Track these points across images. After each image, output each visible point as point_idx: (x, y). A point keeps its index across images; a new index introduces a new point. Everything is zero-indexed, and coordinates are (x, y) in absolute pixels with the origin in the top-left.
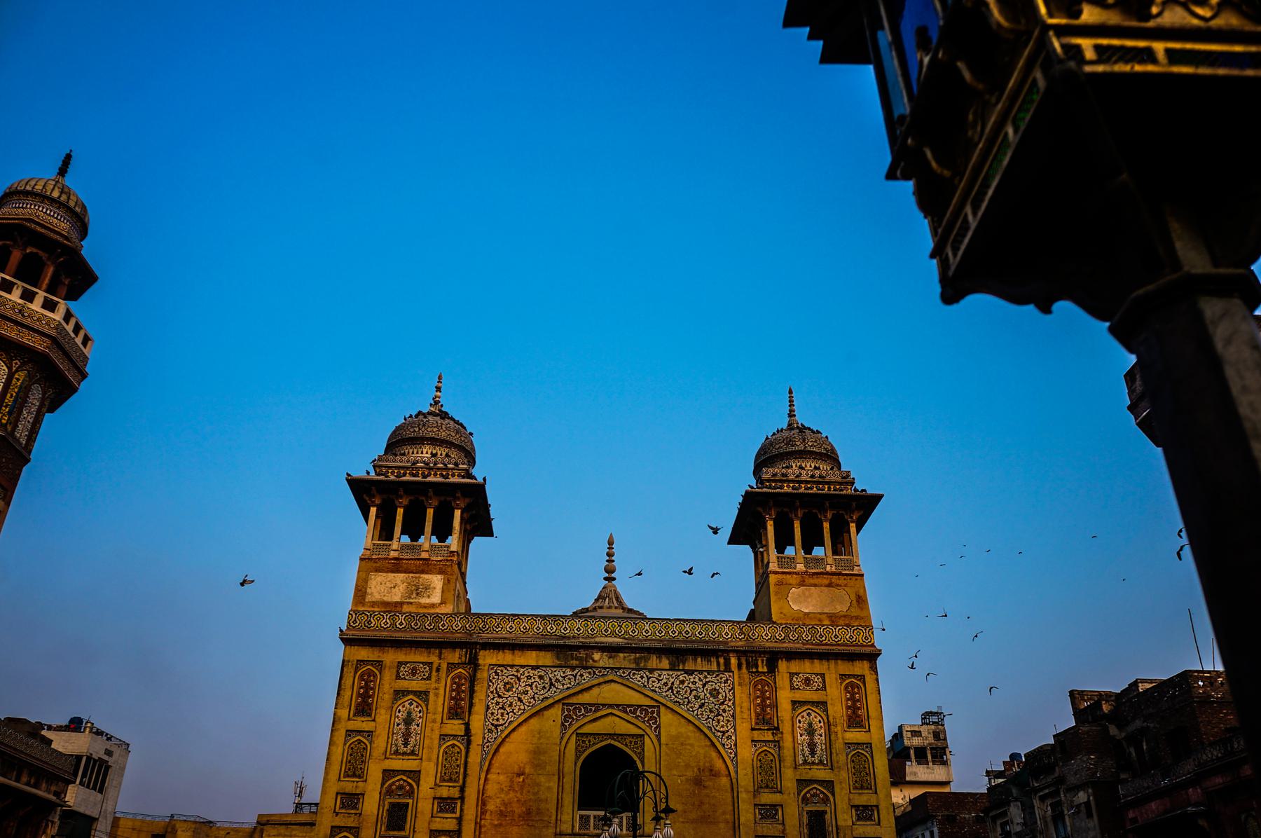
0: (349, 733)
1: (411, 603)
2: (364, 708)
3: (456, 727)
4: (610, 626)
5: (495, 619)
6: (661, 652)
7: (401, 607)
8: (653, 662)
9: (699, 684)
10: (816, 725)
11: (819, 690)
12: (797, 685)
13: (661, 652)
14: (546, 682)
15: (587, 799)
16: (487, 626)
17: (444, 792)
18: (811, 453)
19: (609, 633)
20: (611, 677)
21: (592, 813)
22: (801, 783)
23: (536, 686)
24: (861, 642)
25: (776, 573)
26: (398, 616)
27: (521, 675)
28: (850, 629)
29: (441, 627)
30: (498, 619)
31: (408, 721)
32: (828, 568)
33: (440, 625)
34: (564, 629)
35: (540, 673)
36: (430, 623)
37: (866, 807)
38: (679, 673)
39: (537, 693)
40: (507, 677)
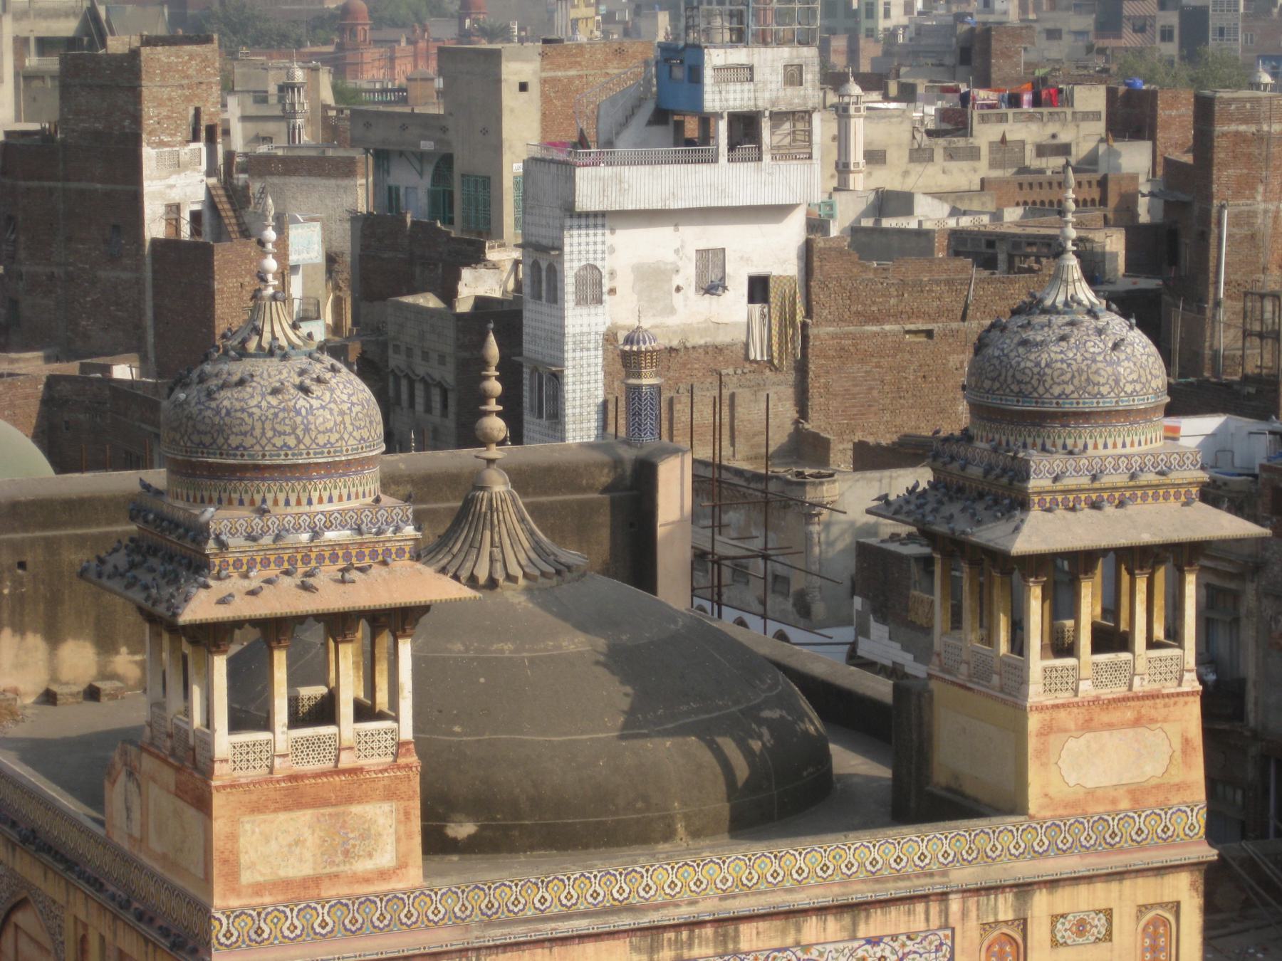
1: (337, 876)
4: (730, 870)
5: (510, 887)
8: (811, 929)
11: (1100, 940)
12: (1063, 937)
16: (496, 905)
18: (1127, 414)
19: (729, 884)
24: (1182, 835)
25: (1041, 709)
26: (315, 909)
28: (1166, 813)
29: (404, 920)
30: (516, 885)
33: (402, 916)
34: (644, 889)
38: (856, 944)
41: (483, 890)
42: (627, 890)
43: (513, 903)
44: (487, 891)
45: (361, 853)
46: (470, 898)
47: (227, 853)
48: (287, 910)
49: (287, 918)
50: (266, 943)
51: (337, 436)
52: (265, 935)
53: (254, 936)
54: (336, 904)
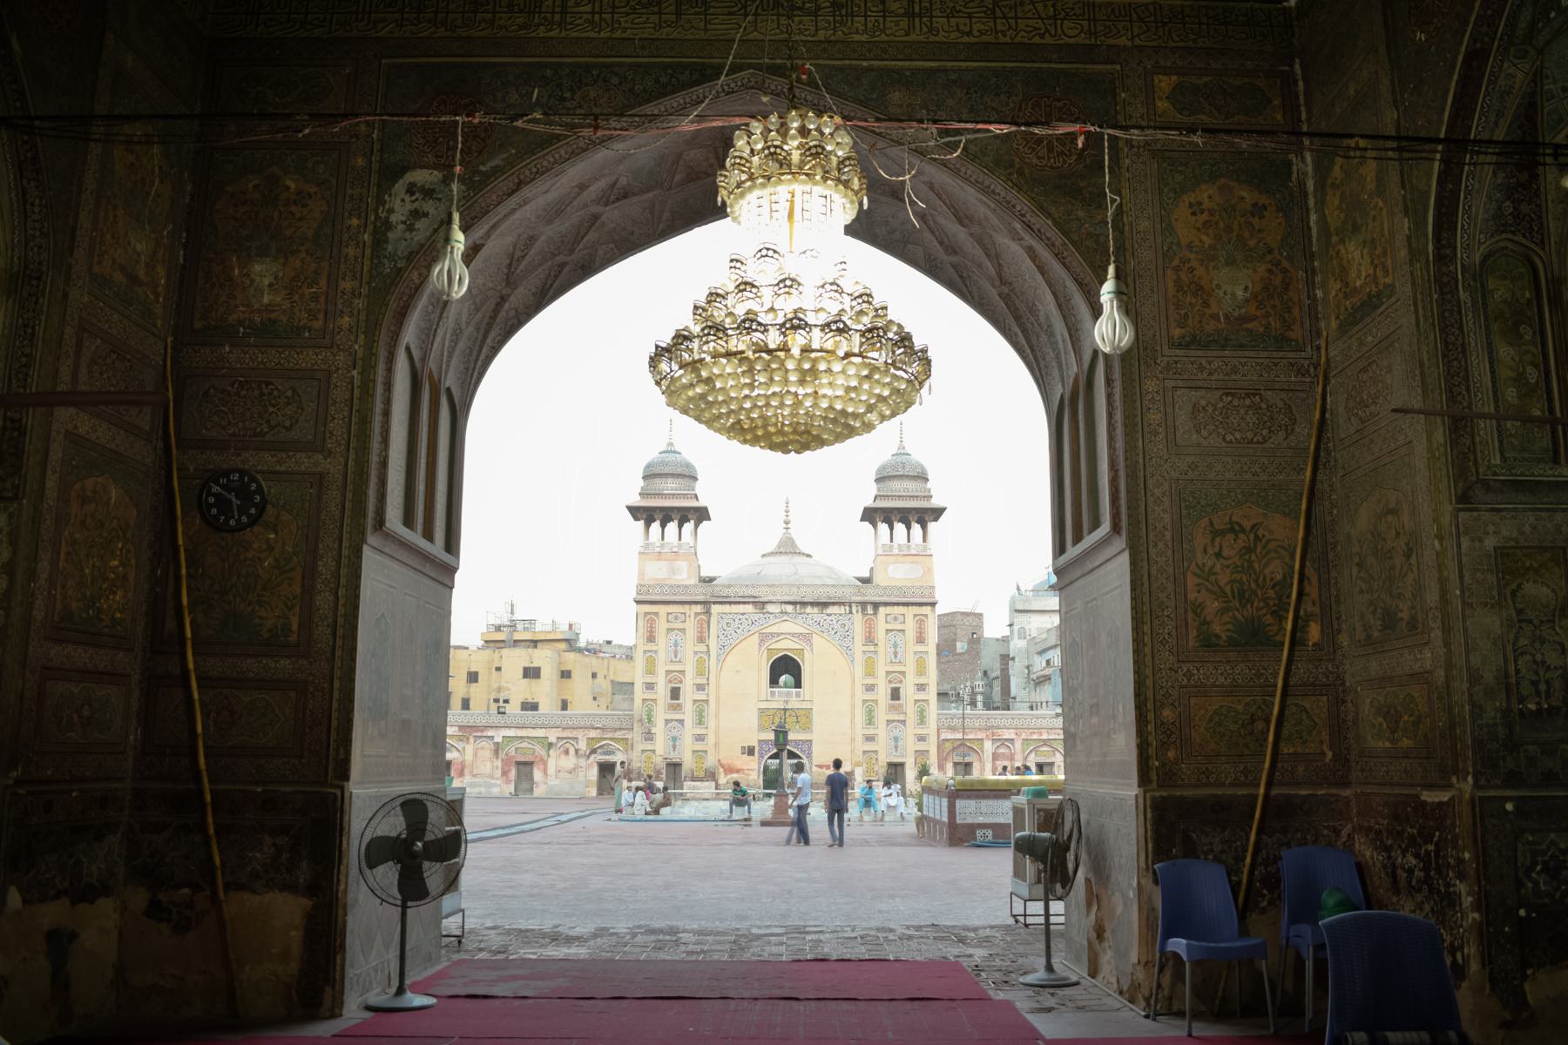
0: (645, 652)
2: (651, 639)
3: (702, 648)
6: (812, 604)
8: (809, 609)
9: (835, 621)
10: (898, 642)
13: (812, 604)
15: (774, 681)
17: (699, 681)
18: (908, 476)
20: (785, 618)
21: (776, 690)
22: (888, 673)
31: (676, 645)
32: (913, 552)
37: (922, 685)
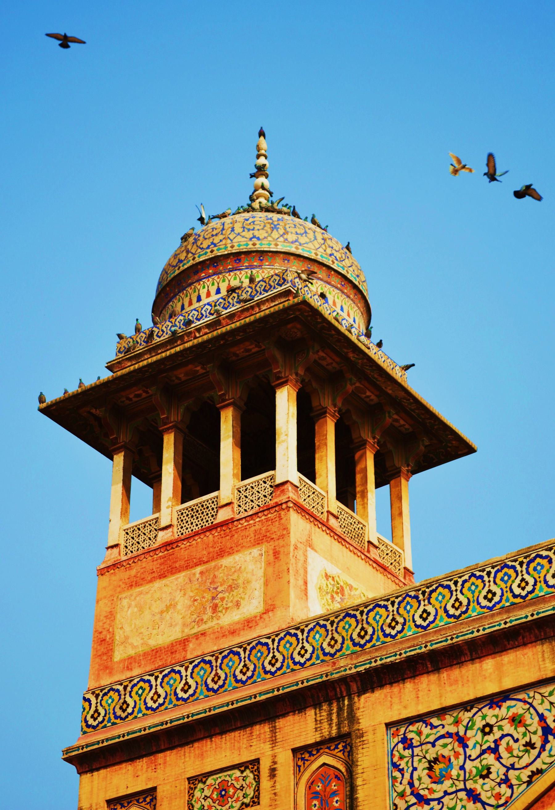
1: (203, 634)
5: (386, 607)
7: (185, 650)
14: (532, 729)
16: (370, 631)
23: (509, 749)
26: (179, 672)
27: (467, 728)
29: (269, 667)
30: (393, 603)
35: (513, 711)
36: (245, 665)
39: (513, 767)
40: (433, 745)
41: (354, 616)
42: (531, 581)
43: (390, 626)
44: (359, 617)
45: (230, 605)
46: (339, 629)
47: (104, 633)
48: (152, 679)
49: (151, 687)
50: (130, 717)
51: (221, 237)
52: (130, 710)
53: (119, 713)
54: (199, 663)
